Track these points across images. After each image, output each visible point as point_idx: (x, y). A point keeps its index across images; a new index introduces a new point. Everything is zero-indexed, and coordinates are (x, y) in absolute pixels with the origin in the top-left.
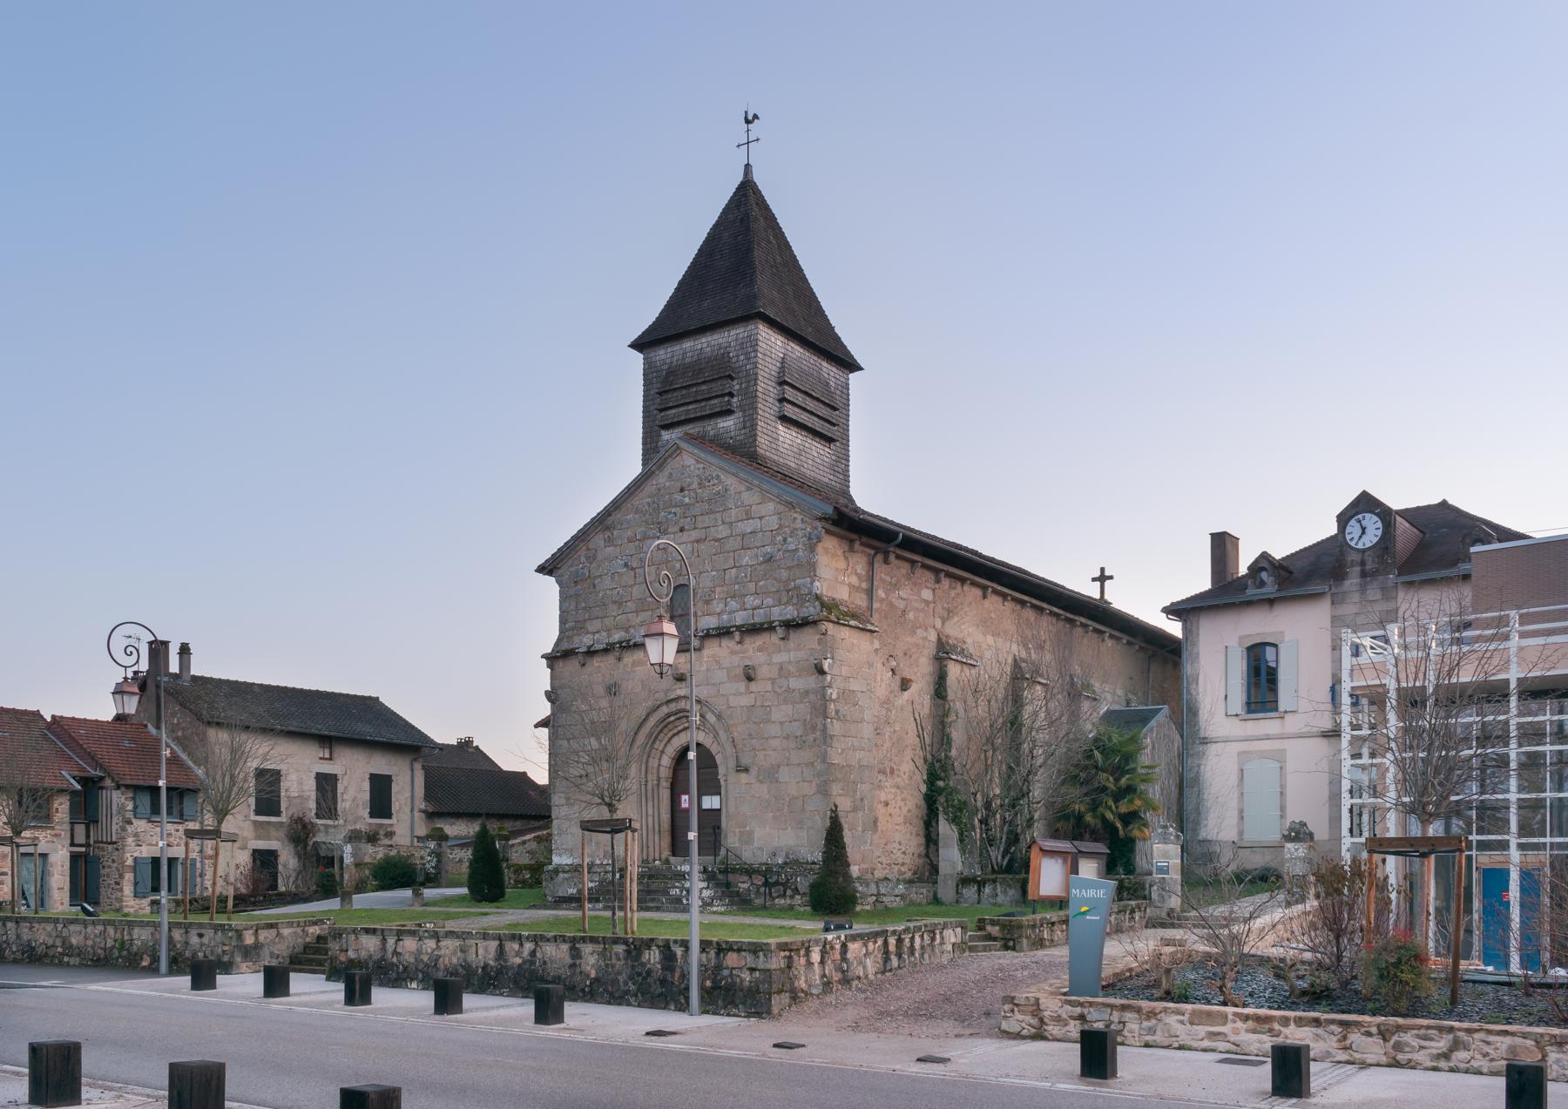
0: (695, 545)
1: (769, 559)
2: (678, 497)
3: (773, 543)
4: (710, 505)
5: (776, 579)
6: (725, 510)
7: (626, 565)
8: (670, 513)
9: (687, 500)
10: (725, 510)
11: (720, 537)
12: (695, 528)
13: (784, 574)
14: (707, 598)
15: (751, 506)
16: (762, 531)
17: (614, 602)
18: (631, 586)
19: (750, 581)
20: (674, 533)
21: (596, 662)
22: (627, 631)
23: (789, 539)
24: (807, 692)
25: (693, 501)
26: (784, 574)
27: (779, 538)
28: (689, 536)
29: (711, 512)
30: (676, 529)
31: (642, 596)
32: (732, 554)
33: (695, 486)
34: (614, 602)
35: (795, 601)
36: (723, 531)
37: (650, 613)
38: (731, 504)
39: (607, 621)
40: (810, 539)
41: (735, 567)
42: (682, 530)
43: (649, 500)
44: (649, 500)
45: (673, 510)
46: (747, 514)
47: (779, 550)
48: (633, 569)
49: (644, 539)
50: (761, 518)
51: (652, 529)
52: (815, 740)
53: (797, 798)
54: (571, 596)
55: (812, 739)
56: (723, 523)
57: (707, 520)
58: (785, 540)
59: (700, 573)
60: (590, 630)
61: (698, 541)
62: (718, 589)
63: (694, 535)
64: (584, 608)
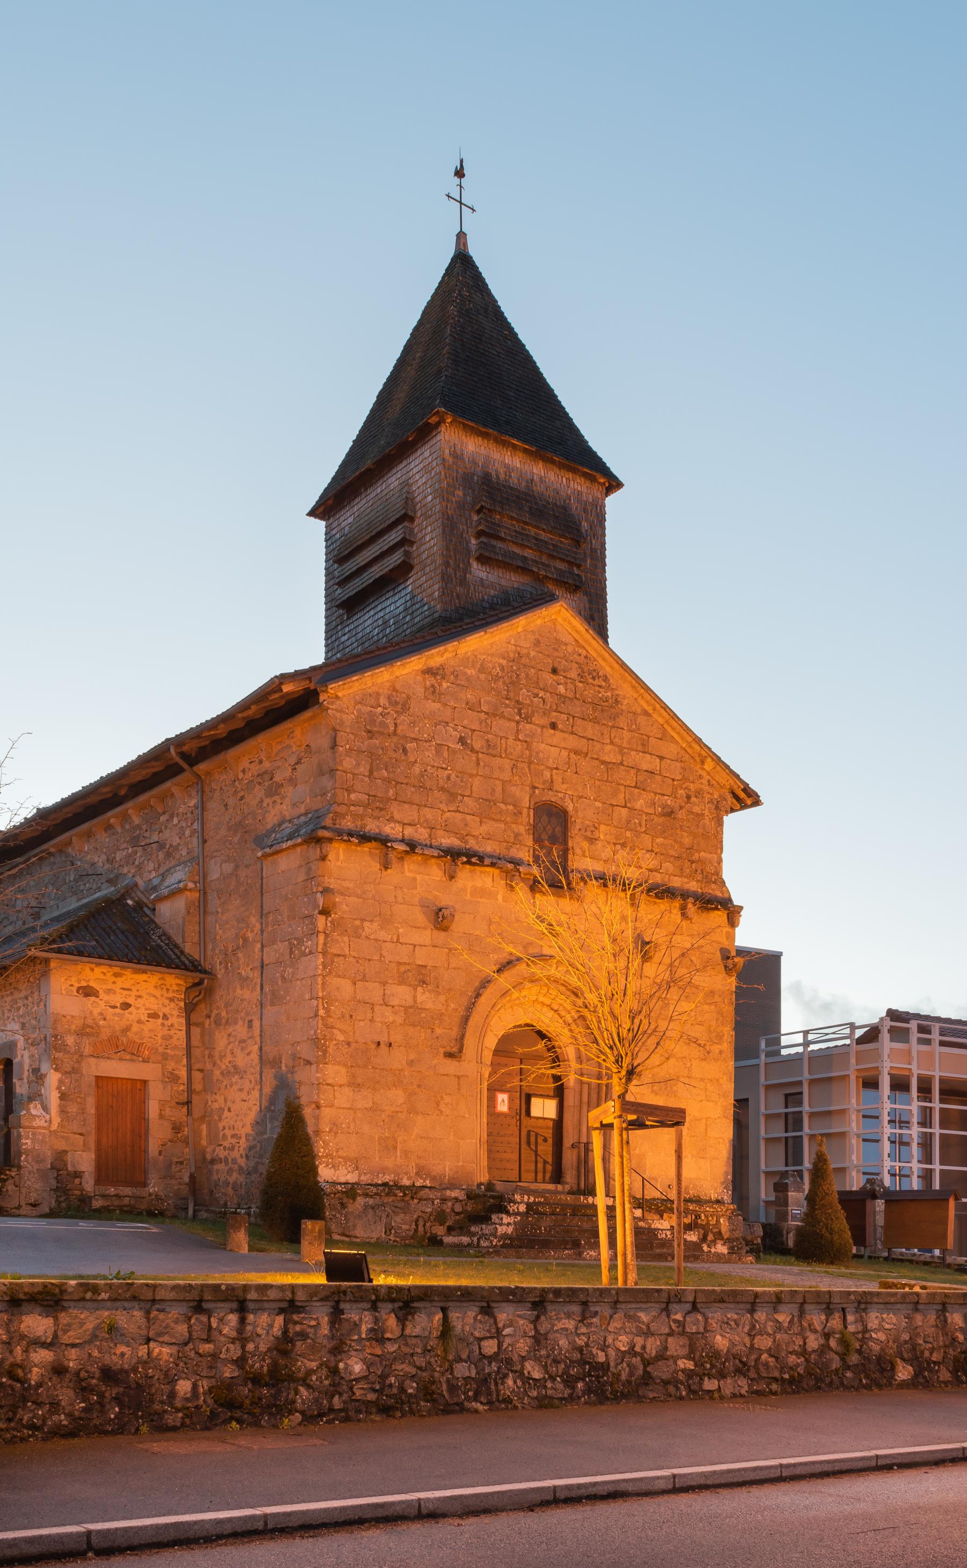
0: (572, 755)
1: (669, 813)
2: (549, 678)
3: (674, 795)
4: (594, 710)
5: (675, 841)
6: (612, 727)
7: (462, 740)
8: (536, 695)
9: (561, 689)
10: (612, 727)
11: (607, 759)
12: (572, 733)
13: (687, 841)
14: (589, 834)
15: (649, 737)
16: (660, 774)
17: (442, 789)
18: (471, 776)
19: (645, 832)
20: (543, 727)
21: (410, 869)
22: (462, 839)
23: (693, 799)
24: (712, 993)
25: (571, 695)
26: (687, 841)
27: (681, 792)
28: (564, 739)
29: (595, 721)
30: (545, 721)
31: (489, 797)
32: (622, 788)
33: (573, 674)
34: (442, 789)
35: (699, 877)
36: (610, 755)
37: (502, 826)
38: (622, 722)
39: (428, 813)
40: (717, 808)
41: (625, 807)
42: (553, 726)
43: (504, 662)
44: (504, 662)
45: (541, 694)
46: (643, 745)
47: (681, 808)
48: (472, 750)
49: (495, 715)
50: (661, 758)
51: (507, 706)
52: (721, 1052)
53: (699, 1120)
54: (360, 751)
55: (717, 1051)
56: (612, 743)
57: (590, 730)
58: (688, 797)
59: (581, 797)
60: (397, 816)
61: (576, 753)
62: (603, 828)
63: (572, 742)
64: (388, 781)
